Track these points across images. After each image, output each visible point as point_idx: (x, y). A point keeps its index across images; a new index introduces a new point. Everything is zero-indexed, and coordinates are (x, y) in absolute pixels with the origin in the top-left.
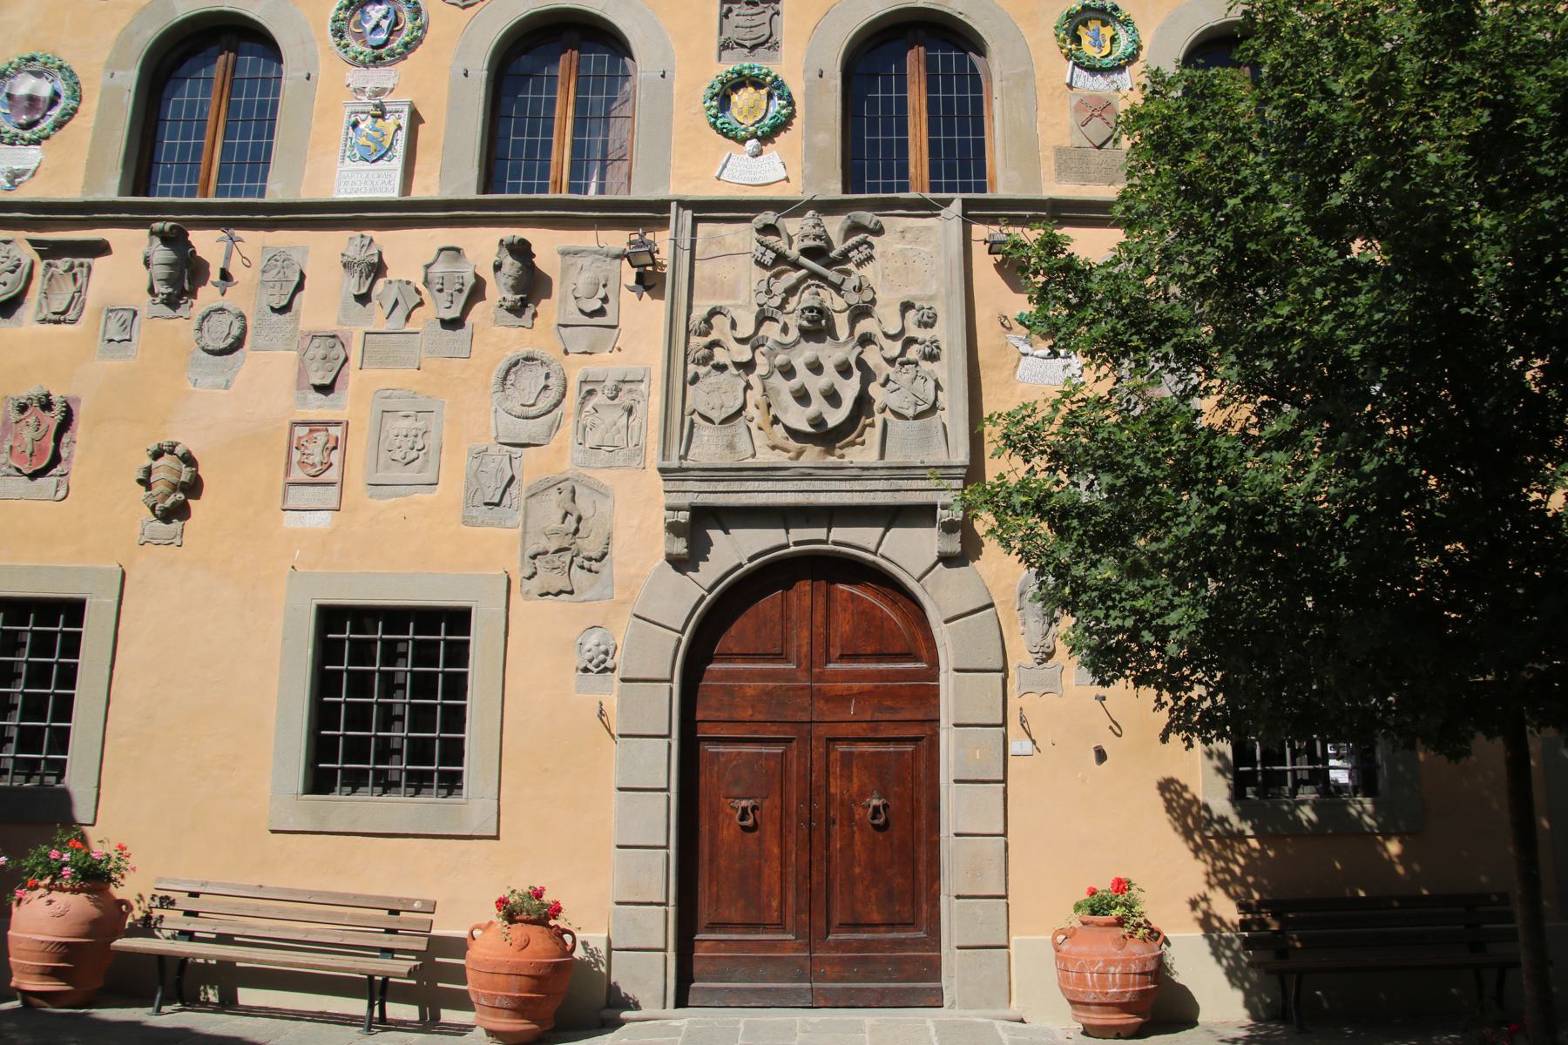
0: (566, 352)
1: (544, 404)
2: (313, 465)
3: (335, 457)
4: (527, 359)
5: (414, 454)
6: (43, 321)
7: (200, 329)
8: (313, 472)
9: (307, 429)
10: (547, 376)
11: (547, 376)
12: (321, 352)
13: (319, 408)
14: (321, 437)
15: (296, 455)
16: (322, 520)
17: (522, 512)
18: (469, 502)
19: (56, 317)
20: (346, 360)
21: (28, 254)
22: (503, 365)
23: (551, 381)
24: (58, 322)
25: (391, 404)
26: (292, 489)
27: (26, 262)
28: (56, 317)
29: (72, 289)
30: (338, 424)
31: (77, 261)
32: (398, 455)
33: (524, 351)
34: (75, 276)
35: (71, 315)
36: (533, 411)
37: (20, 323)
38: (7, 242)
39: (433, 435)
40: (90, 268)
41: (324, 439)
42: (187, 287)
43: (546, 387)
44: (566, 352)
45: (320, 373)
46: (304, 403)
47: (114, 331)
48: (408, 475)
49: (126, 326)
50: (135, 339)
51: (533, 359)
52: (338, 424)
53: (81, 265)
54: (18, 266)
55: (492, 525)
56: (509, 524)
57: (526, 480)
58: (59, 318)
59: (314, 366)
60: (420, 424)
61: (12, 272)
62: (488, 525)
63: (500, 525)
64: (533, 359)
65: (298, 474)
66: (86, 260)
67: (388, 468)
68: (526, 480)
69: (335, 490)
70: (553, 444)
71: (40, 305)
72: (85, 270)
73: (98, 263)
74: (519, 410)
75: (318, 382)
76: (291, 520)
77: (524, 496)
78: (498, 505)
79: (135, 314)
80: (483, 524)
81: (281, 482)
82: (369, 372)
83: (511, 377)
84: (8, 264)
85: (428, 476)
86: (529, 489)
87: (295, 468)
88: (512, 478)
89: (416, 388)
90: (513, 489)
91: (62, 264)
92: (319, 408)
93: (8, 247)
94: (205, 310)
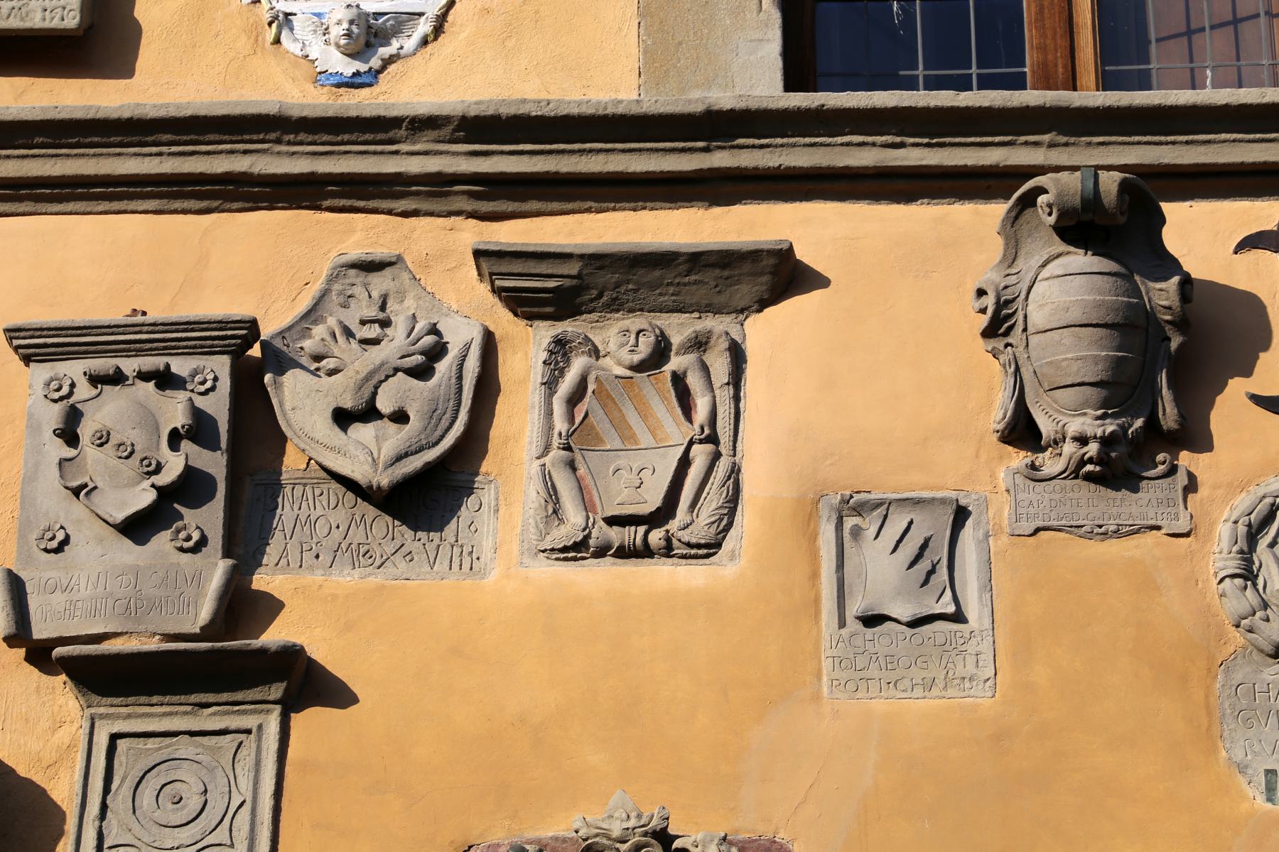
6: (577, 550)
7: (1248, 574)
19: (633, 535)
21: (464, 307)
24: (645, 552)
27: (461, 334)
28: (633, 535)
29: (676, 432)
31: (679, 328)
34: (679, 381)
35: (691, 523)
37: (469, 561)
38: (370, 267)
40: (737, 355)
42: (1169, 415)
47: (881, 572)
49: (933, 562)
50: (973, 610)
53: (699, 344)
54: (437, 352)
58: (643, 534)
61: (422, 372)
66: (716, 324)
71: (552, 494)
72: (720, 366)
73: (769, 332)
79: (961, 515)
84: (396, 343)
91: (616, 339)
93: (380, 283)
94: (1243, 503)
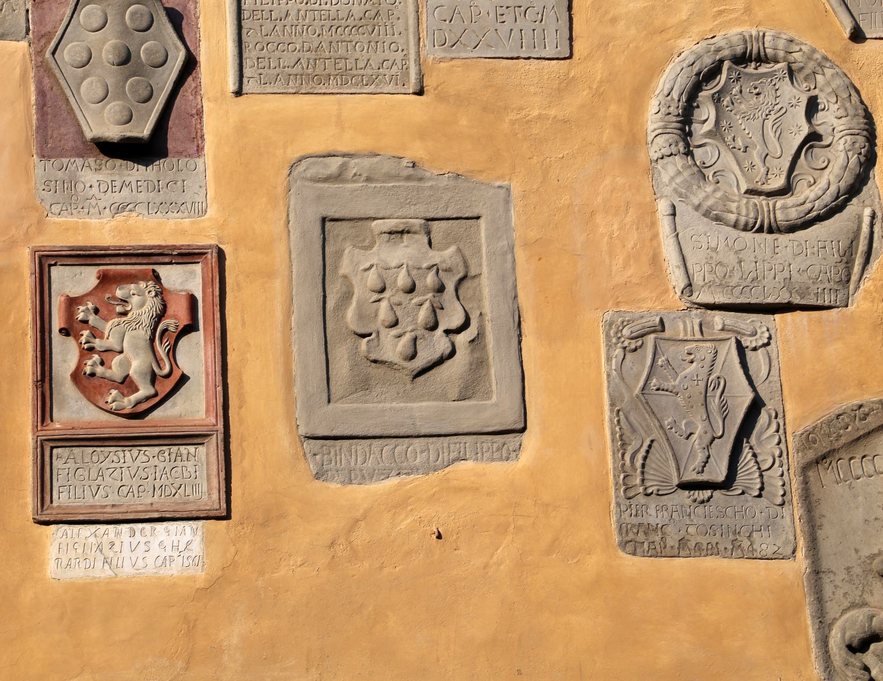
0: (857, 36)
1: (816, 187)
2: (126, 384)
3: (195, 355)
4: (741, 59)
5: (439, 343)
8: (128, 402)
9: (85, 279)
10: (812, 107)
11: (812, 107)
12: (107, 46)
13: (115, 210)
14: (141, 301)
15: (66, 356)
16: (171, 552)
17: (798, 509)
18: (634, 477)
20: (190, 64)
22: (672, 79)
23: (830, 119)
25: (347, 200)
26: (64, 461)
30: (187, 256)
32: (392, 348)
33: (732, 34)
36: (787, 209)
39: (487, 286)
41: (151, 304)
43: (813, 138)
44: (857, 36)
45: (114, 107)
46: (69, 195)
48: (422, 409)
51: (761, 59)
52: (187, 256)
55: (713, 551)
56: (764, 544)
57: (798, 410)
59: (90, 88)
60: (446, 255)
62: (699, 551)
63: (738, 548)
64: (761, 59)
65: (74, 410)
67: (363, 385)
68: (798, 410)
69: (205, 456)
70: (860, 303)
74: (743, 208)
75: (113, 132)
76: (69, 556)
77: (795, 460)
78: (727, 484)
80: (683, 548)
81: (29, 440)
82: (267, 106)
83: (706, 112)
85: (497, 407)
86: (808, 439)
87: (66, 391)
88: (756, 406)
89: (416, 151)
90: (764, 441)
92: (115, 210)
